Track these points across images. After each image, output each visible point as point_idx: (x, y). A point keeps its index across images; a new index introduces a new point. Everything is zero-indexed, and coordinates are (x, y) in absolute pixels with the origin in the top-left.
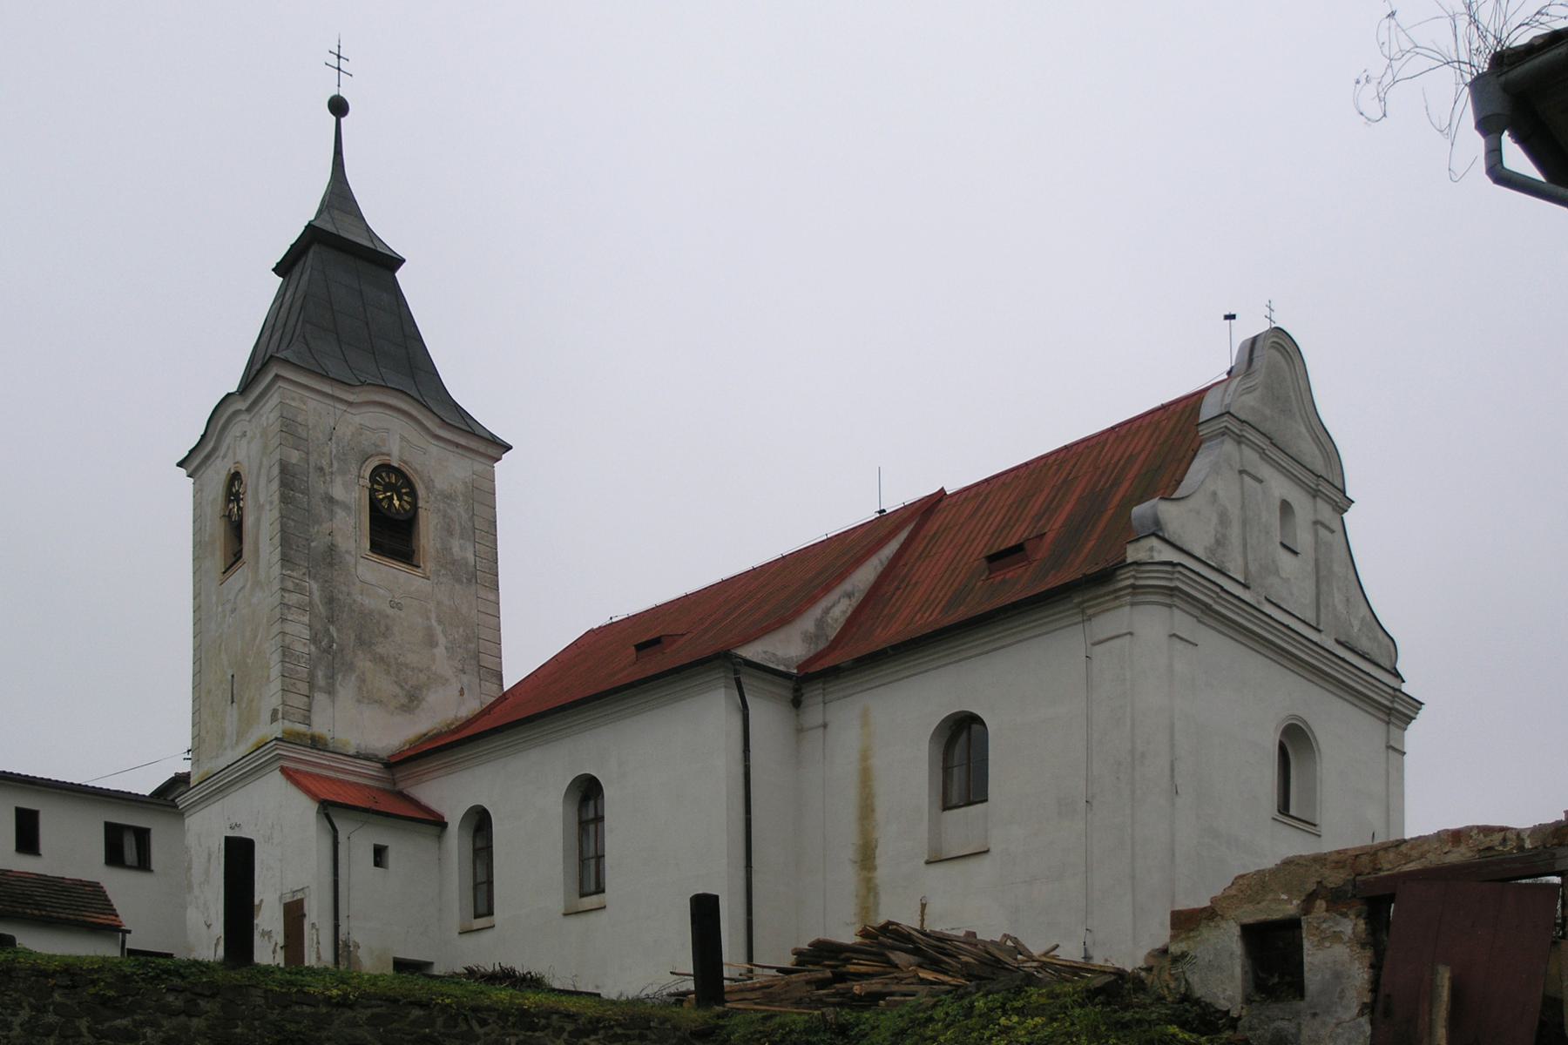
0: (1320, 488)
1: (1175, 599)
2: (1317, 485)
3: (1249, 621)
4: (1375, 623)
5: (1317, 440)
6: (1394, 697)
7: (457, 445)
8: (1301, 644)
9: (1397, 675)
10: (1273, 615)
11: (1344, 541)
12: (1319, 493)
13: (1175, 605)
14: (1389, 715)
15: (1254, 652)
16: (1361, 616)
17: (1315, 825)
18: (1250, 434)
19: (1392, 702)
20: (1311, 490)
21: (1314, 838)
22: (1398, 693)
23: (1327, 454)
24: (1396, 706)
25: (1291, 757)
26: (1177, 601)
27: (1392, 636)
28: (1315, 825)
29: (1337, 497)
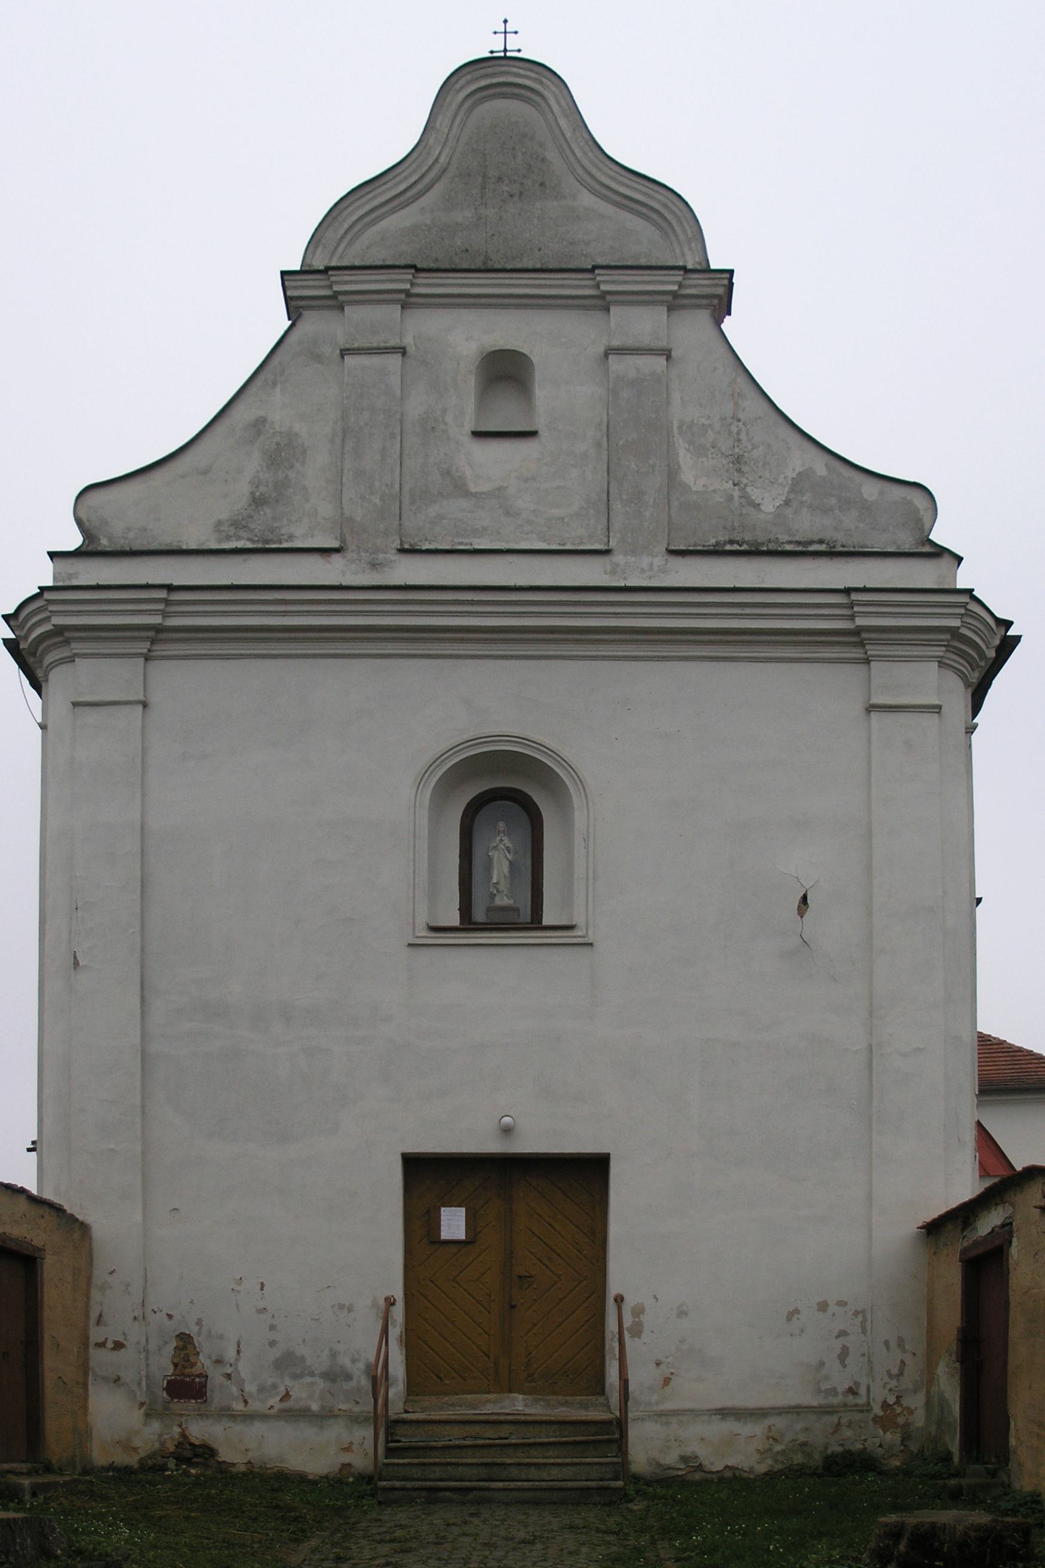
0: (603, 287)
1: (73, 645)
2: (598, 286)
3: (285, 613)
4: (846, 472)
5: (627, 203)
6: (851, 606)
7: (636, 641)
8: (472, 603)
9: (939, 552)
10: (150, 582)
11: (724, 349)
12: (609, 298)
13: (76, 655)
14: (862, 644)
15: (302, 661)
16: (791, 474)
17: (570, 928)
18: (346, 283)
19: (852, 618)
20: (593, 302)
21: (585, 949)
22: (854, 596)
23: (582, 184)
24: (860, 621)
25: (537, 800)
26: (77, 647)
27: (912, 480)
28: (570, 928)
29: (699, 285)
